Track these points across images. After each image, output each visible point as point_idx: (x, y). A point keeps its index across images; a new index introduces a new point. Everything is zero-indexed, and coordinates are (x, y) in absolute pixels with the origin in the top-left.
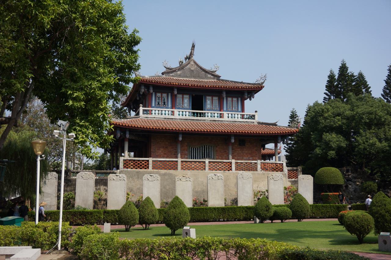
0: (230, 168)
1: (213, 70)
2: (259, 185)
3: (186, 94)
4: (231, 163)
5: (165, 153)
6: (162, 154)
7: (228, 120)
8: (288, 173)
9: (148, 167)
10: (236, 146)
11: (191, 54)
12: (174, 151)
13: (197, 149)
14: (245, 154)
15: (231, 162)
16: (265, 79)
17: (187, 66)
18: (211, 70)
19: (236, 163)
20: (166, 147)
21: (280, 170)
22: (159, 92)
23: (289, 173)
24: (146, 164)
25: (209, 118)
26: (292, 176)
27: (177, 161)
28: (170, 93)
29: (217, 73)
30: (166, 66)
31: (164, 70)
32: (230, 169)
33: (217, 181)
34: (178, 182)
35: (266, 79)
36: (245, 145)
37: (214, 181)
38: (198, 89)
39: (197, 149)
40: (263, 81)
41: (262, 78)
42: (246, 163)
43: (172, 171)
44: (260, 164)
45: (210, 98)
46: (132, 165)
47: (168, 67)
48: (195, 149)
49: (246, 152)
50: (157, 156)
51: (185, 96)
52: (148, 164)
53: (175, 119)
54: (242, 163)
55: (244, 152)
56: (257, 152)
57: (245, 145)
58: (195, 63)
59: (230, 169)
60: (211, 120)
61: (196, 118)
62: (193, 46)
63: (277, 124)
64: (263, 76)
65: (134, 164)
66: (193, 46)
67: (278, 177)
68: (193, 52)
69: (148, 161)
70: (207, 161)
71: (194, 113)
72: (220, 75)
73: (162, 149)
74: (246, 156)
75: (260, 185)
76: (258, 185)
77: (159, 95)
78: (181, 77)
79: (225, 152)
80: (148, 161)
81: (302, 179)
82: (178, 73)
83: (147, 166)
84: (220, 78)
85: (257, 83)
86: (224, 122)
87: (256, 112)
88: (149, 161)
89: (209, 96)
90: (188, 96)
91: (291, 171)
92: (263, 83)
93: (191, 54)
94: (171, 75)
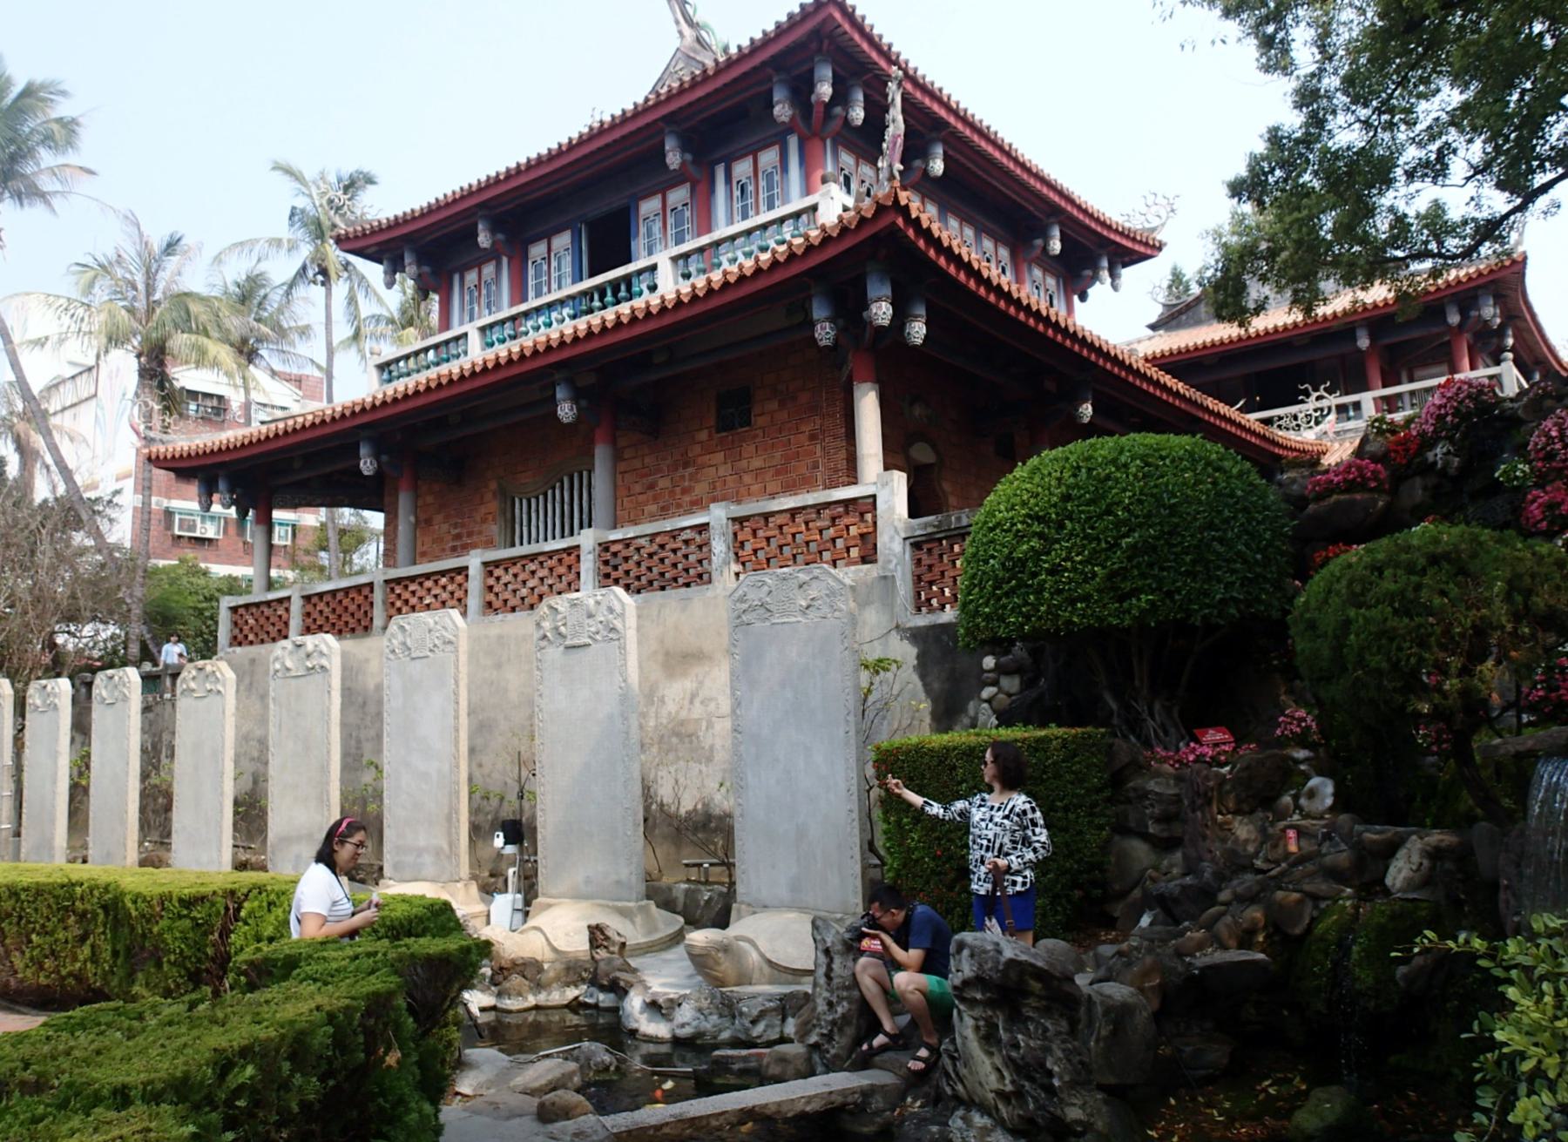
2: (701, 683)
3: (558, 230)
8: (918, 562)
10: (703, 435)
14: (747, 479)
15: (578, 547)
23: (926, 560)
33: (303, 679)
36: (749, 424)
37: (293, 682)
44: (731, 528)
48: (524, 502)
49: (757, 463)
55: (744, 463)
56: (818, 454)
57: (749, 424)
67: (590, 616)
70: (474, 561)
74: (755, 488)
75: (708, 683)
76: (695, 685)
79: (652, 486)
81: (753, 609)
89: (648, 195)
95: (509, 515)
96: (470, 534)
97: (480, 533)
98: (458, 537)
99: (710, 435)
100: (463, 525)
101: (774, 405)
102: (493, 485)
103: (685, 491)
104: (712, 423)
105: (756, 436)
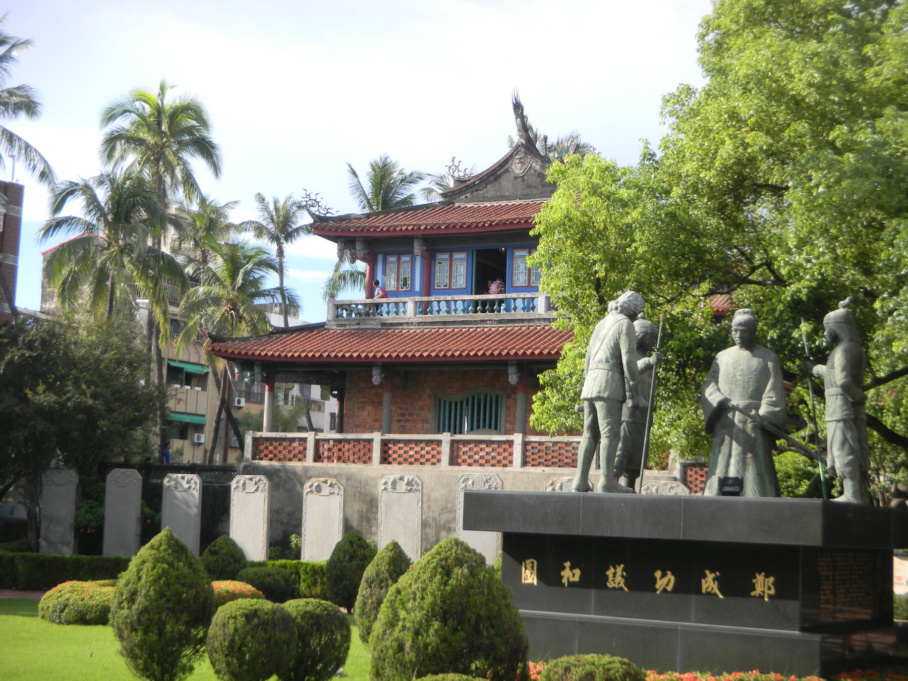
3: (460, 251)
5: (376, 417)
6: (370, 420)
7: (547, 316)
11: (525, 128)
12: (399, 412)
13: (459, 404)
19: (525, 444)
21: (492, 462)
22: (392, 254)
26: (698, 482)
27: (370, 441)
34: (310, 496)
38: (438, 234)
39: (459, 404)
42: (555, 443)
43: (355, 468)
46: (271, 452)
47: (461, 174)
50: (357, 426)
51: (457, 256)
54: (540, 443)
60: (501, 320)
61: (480, 316)
62: (518, 107)
66: (518, 107)
71: (476, 303)
73: (369, 408)
77: (392, 259)
80: (304, 440)
88: (308, 439)
90: (463, 255)
91: (694, 469)
95: (437, 408)
96: (411, 415)
97: (418, 415)
98: (403, 415)
100: (407, 409)
102: (428, 391)
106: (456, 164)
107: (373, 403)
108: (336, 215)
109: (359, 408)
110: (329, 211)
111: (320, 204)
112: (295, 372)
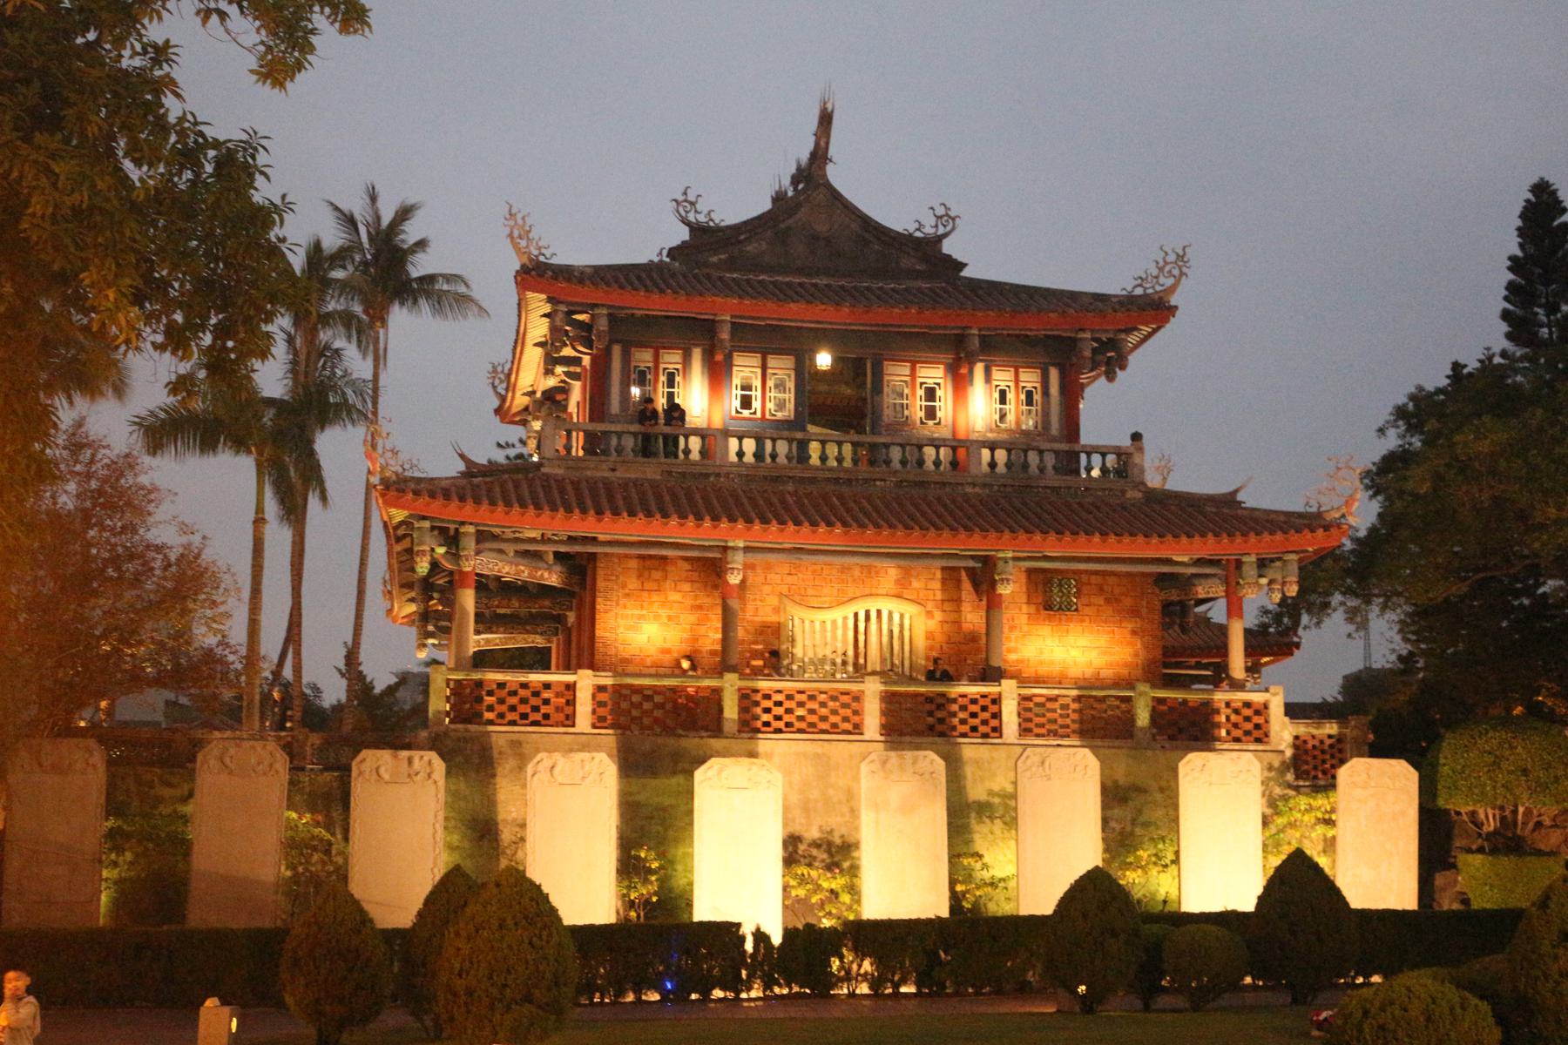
0: (994, 723)
1: (929, 230)
3: (780, 352)
4: (997, 701)
9: (570, 720)
11: (819, 156)
16: (1176, 272)
17: (798, 216)
18: (918, 234)
20: (670, 618)
22: (642, 345)
24: (563, 700)
25: (896, 472)
28: (697, 345)
29: (948, 247)
30: (691, 217)
31: (683, 234)
32: (994, 729)
35: (1184, 269)
40: (1170, 281)
41: (1167, 268)
45: (905, 370)
47: (702, 218)
51: (773, 362)
52: (571, 702)
53: (718, 475)
55: (1071, 639)
58: (836, 196)
59: (994, 729)
62: (826, 119)
63: (1240, 497)
64: (1172, 258)
65: (501, 701)
66: (826, 119)
68: (822, 144)
69: (571, 687)
72: (964, 261)
78: (762, 272)
80: (571, 687)
82: (749, 248)
83: (568, 710)
84: (965, 273)
85: (1139, 291)
86: (969, 490)
87: (1136, 437)
88: (578, 686)
92: (1172, 289)
93: (819, 156)
94: (714, 259)
99: (1038, 610)
101: (1101, 601)
103: (1009, 651)
104: (1040, 600)
105: (1083, 621)
106: (691, 198)
107: (657, 617)
108: (554, 261)
109: (630, 628)
110: (543, 251)
111: (531, 236)
112: (501, 551)
